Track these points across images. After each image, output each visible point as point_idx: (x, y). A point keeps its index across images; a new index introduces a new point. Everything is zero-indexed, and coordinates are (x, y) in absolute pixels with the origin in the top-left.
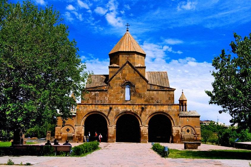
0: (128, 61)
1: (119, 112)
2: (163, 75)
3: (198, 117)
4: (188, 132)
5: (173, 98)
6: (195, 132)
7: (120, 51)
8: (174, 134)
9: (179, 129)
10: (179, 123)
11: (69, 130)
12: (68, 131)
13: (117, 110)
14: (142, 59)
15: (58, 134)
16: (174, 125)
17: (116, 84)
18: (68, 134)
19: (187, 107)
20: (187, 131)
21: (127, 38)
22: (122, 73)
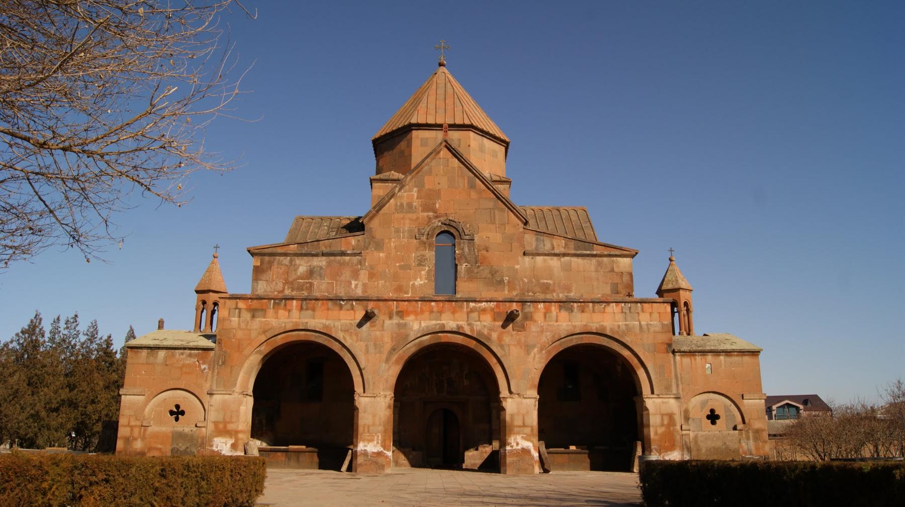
0: (446, 141)
1: (407, 336)
2: (574, 218)
3: (755, 353)
4: (713, 423)
5: (630, 287)
6: (744, 422)
7: (414, 121)
8: (652, 430)
9: (672, 405)
10: (674, 381)
11: (183, 413)
12: (177, 419)
13: (399, 325)
14: (494, 154)
15: (132, 431)
16: (653, 393)
17: (397, 231)
18: (176, 429)
19: (693, 316)
20: (708, 417)
21: (442, 86)
22: (420, 186)
